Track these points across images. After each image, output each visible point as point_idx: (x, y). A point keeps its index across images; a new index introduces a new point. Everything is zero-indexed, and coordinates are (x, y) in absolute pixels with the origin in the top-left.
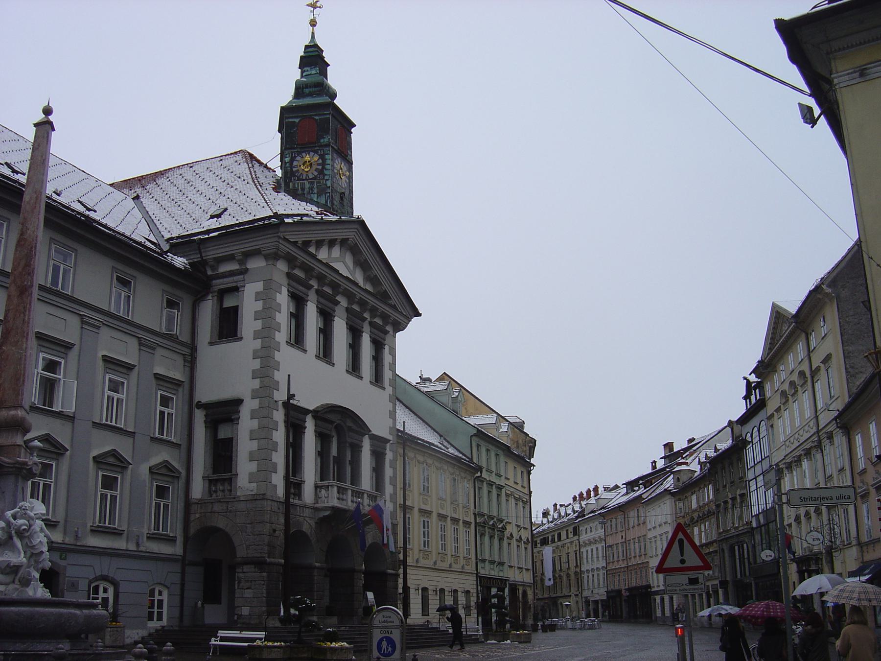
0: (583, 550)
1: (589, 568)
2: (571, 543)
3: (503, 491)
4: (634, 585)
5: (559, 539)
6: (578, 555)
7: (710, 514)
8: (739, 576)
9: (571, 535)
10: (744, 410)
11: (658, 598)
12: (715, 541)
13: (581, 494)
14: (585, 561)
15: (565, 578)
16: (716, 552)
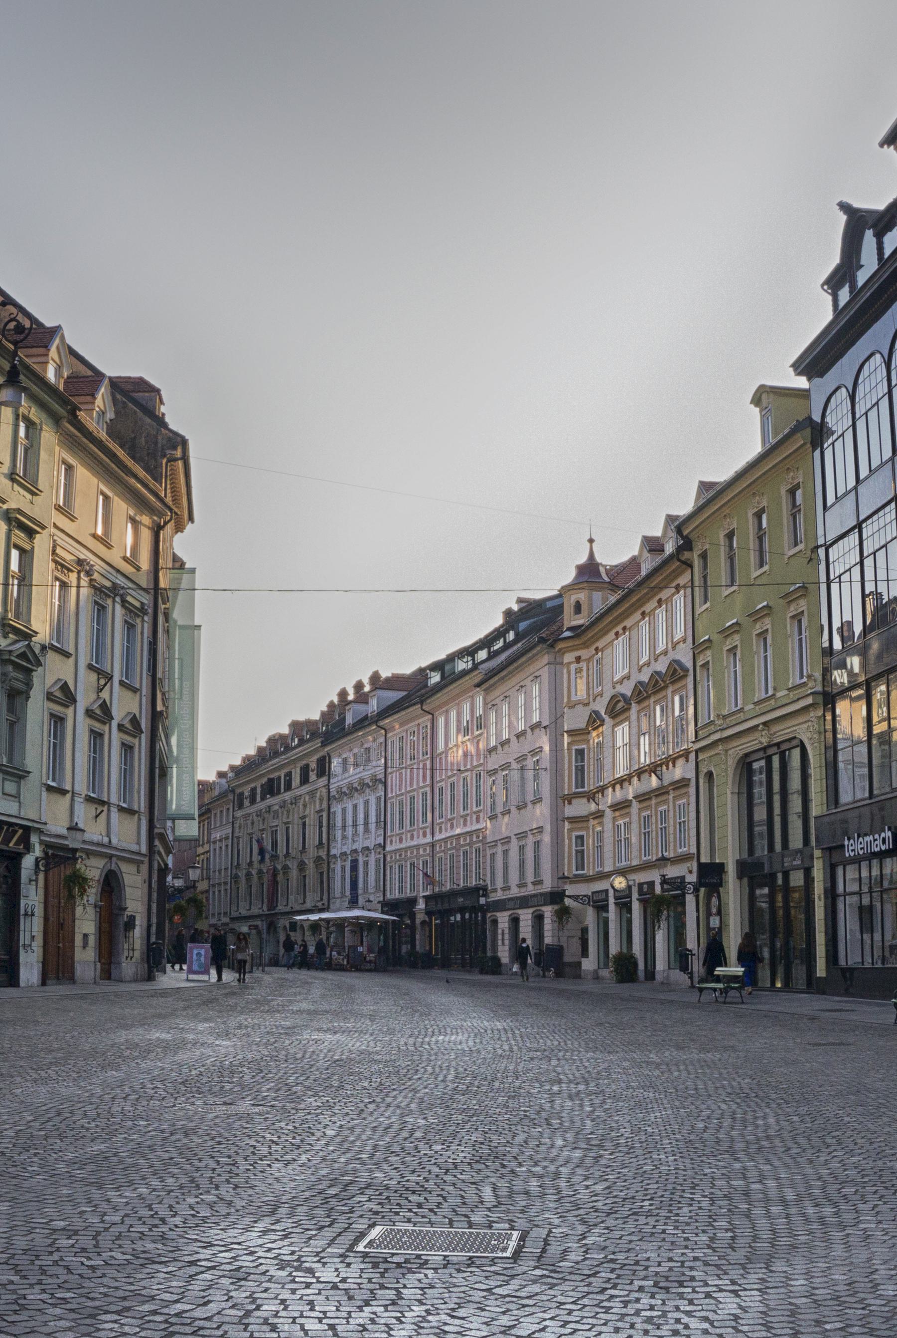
0: (337, 808)
1: (347, 849)
2: (312, 793)
3: (41, 544)
4: (448, 887)
5: (288, 787)
6: (326, 823)
7: (676, 674)
8: (761, 851)
9: (313, 776)
10: (829, 316)
11: (503, 919)
12: (686, 755)
13: (343, 694)
14: (339, 834)
15: (294, 873)
16: (682, 784)
